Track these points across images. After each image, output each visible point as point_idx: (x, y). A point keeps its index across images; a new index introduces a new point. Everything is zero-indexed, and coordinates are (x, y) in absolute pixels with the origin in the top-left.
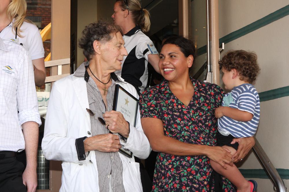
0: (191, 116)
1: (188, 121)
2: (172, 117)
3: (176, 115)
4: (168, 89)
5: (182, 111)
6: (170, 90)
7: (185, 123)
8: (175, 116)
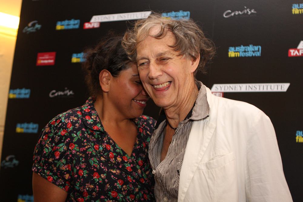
0: (139, 175)
1: (135, 185)
2: (108, 177)
3: (114, 174)
4: (98, 123)
5: (124, 167)
6: (102, 126)
7: (129, 188)
8: (112, 176)
